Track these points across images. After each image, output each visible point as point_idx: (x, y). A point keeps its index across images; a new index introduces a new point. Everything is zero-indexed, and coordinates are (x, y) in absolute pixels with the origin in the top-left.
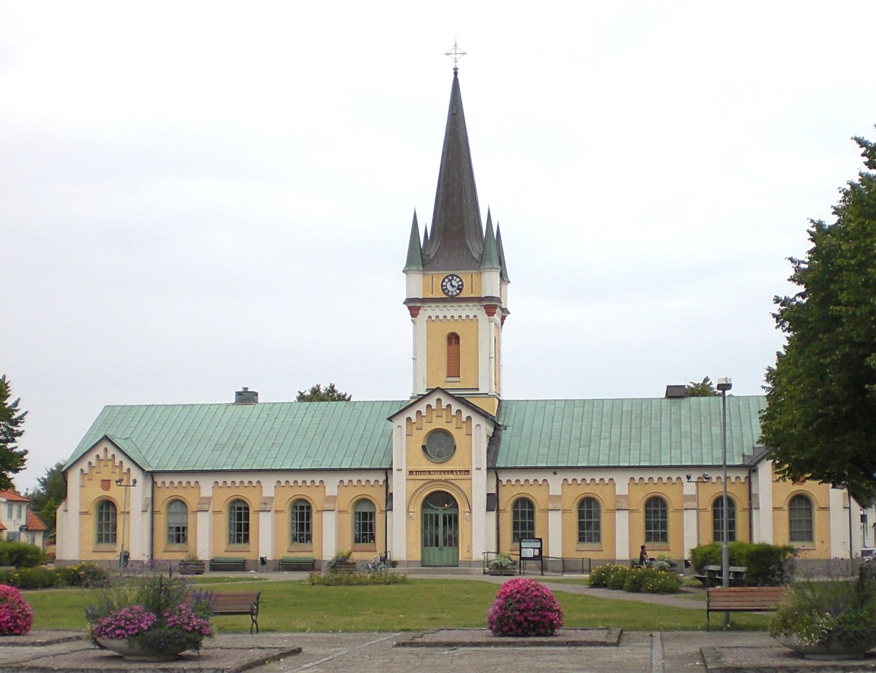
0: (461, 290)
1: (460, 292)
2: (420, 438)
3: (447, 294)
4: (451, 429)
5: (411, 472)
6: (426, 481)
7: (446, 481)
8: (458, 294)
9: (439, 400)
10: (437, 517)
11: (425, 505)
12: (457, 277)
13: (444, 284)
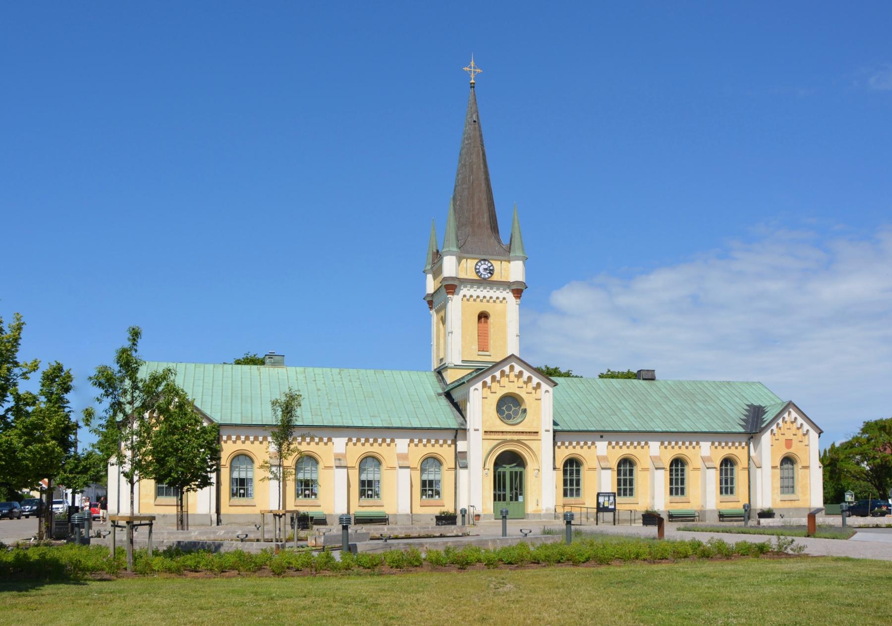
0: (492, 274)
1: (491, 276)
2: (494, 399)
3: (480, 276)
4: (522, 393)
5: (485, 432)
6: (500, 441)
7: (518, 441)
8: (489, 277)
9: (512, 368)
10: (504, 473)
11: (497, 464)
12: (489, 262)
13: (478, 267)
